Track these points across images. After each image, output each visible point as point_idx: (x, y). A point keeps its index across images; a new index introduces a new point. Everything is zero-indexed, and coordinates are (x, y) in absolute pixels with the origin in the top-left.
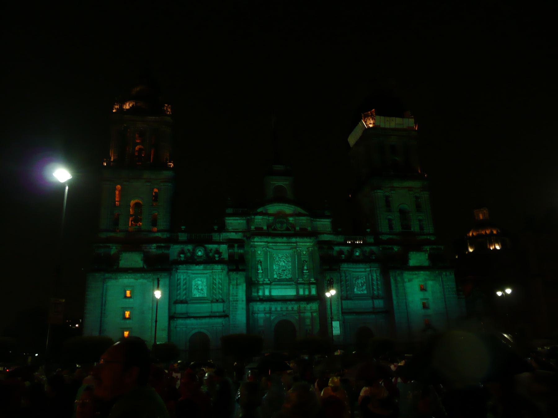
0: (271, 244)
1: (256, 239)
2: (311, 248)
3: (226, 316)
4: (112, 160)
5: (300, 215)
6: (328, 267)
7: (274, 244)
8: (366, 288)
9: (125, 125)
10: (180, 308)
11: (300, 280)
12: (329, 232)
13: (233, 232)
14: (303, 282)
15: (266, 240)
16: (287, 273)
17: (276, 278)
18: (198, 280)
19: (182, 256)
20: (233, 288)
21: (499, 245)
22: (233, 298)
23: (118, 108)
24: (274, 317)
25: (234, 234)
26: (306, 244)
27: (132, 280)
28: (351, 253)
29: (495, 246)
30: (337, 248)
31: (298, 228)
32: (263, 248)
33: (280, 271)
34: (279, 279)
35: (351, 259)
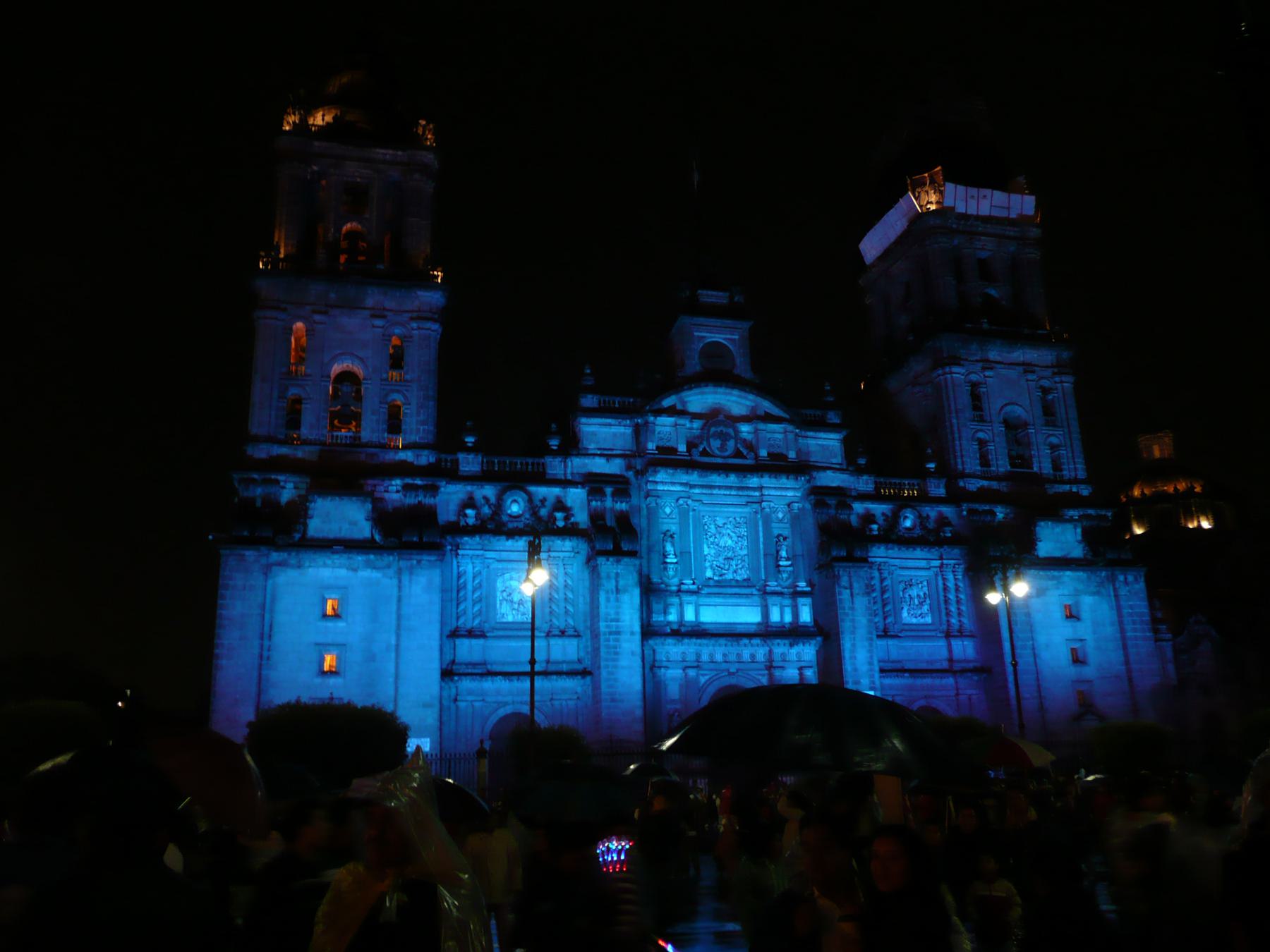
0: (697, 491)
1: (662, 475)
2: (796, 505)
3: (584, 673)
4: (282, 256)
5: (768, 418)
6: (844, 553)
7: (704, 491)
8: (931, 609)
9: (315, 168)
10: (467, 650)
11: (773, 585)
12: (838, 466)
13: (601, 455)
14: (778, 589)
15: (683, 477)
16: (736, 565)
17: (710, 579)
19: (470, 512)
20: (608, 600)
21: (1208, 519)
22: (608, 627)
23: (297, 121)
24: (707, 677)
25: (602, 461)
26: (784, 494)
28: (894, 519)
29: (1199, 522)
30: (859, 507)
31: (763, 453)
32: (677, 500)
33: (721, 559)
34: (718, 581)
35: (892, 536)
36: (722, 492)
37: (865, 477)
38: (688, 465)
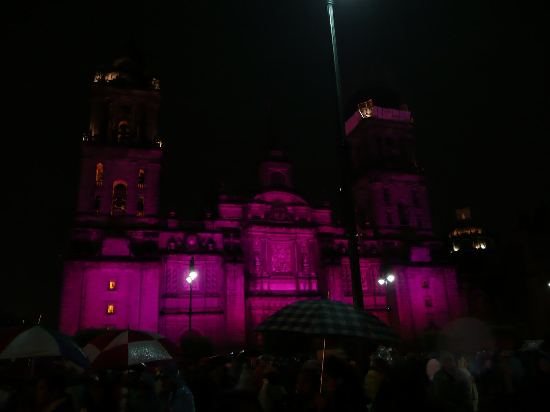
0: (269, 235)
1: (254, 228)
2: (311, 240)
3: (221, 312)
4: (93, 135)
7: (272, 235)
9: (108, 98)
10: (170, 303)
11: (301, 274)
13: (228, 220)
14: (303, 276)
15: (264, 229)
16: (286, 266)
17: (274, 272)
19: (172, 244)
21: (484, 245)
23: (100, 78)
25: (229, 222)
26: (305, 236)
29: (480, 246)
30: (337, 241)
31: (297, 219)
32: (261, 239)
36: (279, 235)
37: (340, 229)
38: (264, 224)
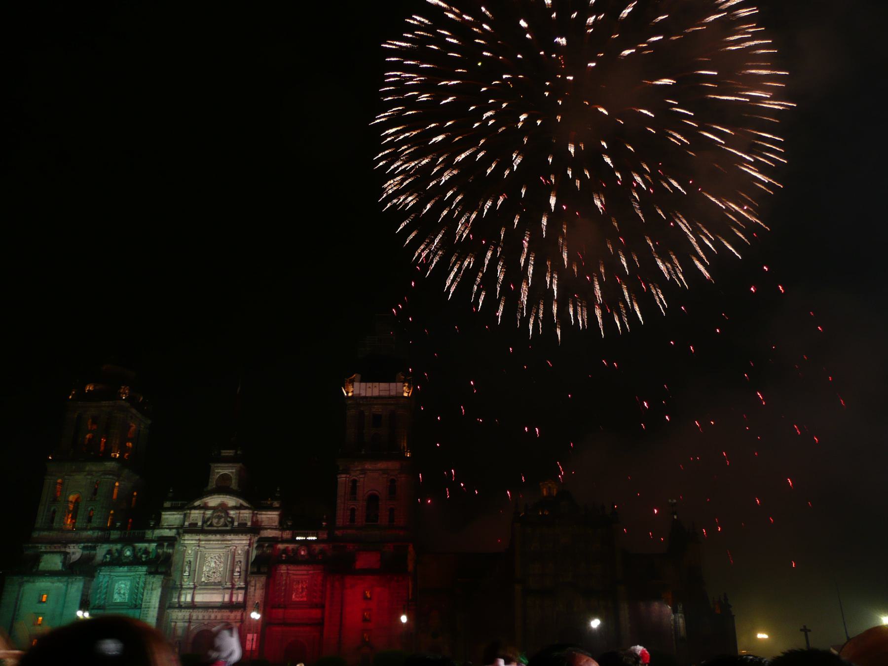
0: (203, 542)
1: (187, 537)
5: (246, 508)
7: (206, 542)
15: (197, 537)
17: (204, 582)
18: (122, 584)
20: (147, 593)
24: (194, 626)
25: (167, 531)
26: (241, 542)
27: (49, 584)
30: (281, 546)
31: (236, 524)
33: (211, 572)
34: (206, 583)
36: (214, 543)
37: (288, 531)
38: (202, 531)
